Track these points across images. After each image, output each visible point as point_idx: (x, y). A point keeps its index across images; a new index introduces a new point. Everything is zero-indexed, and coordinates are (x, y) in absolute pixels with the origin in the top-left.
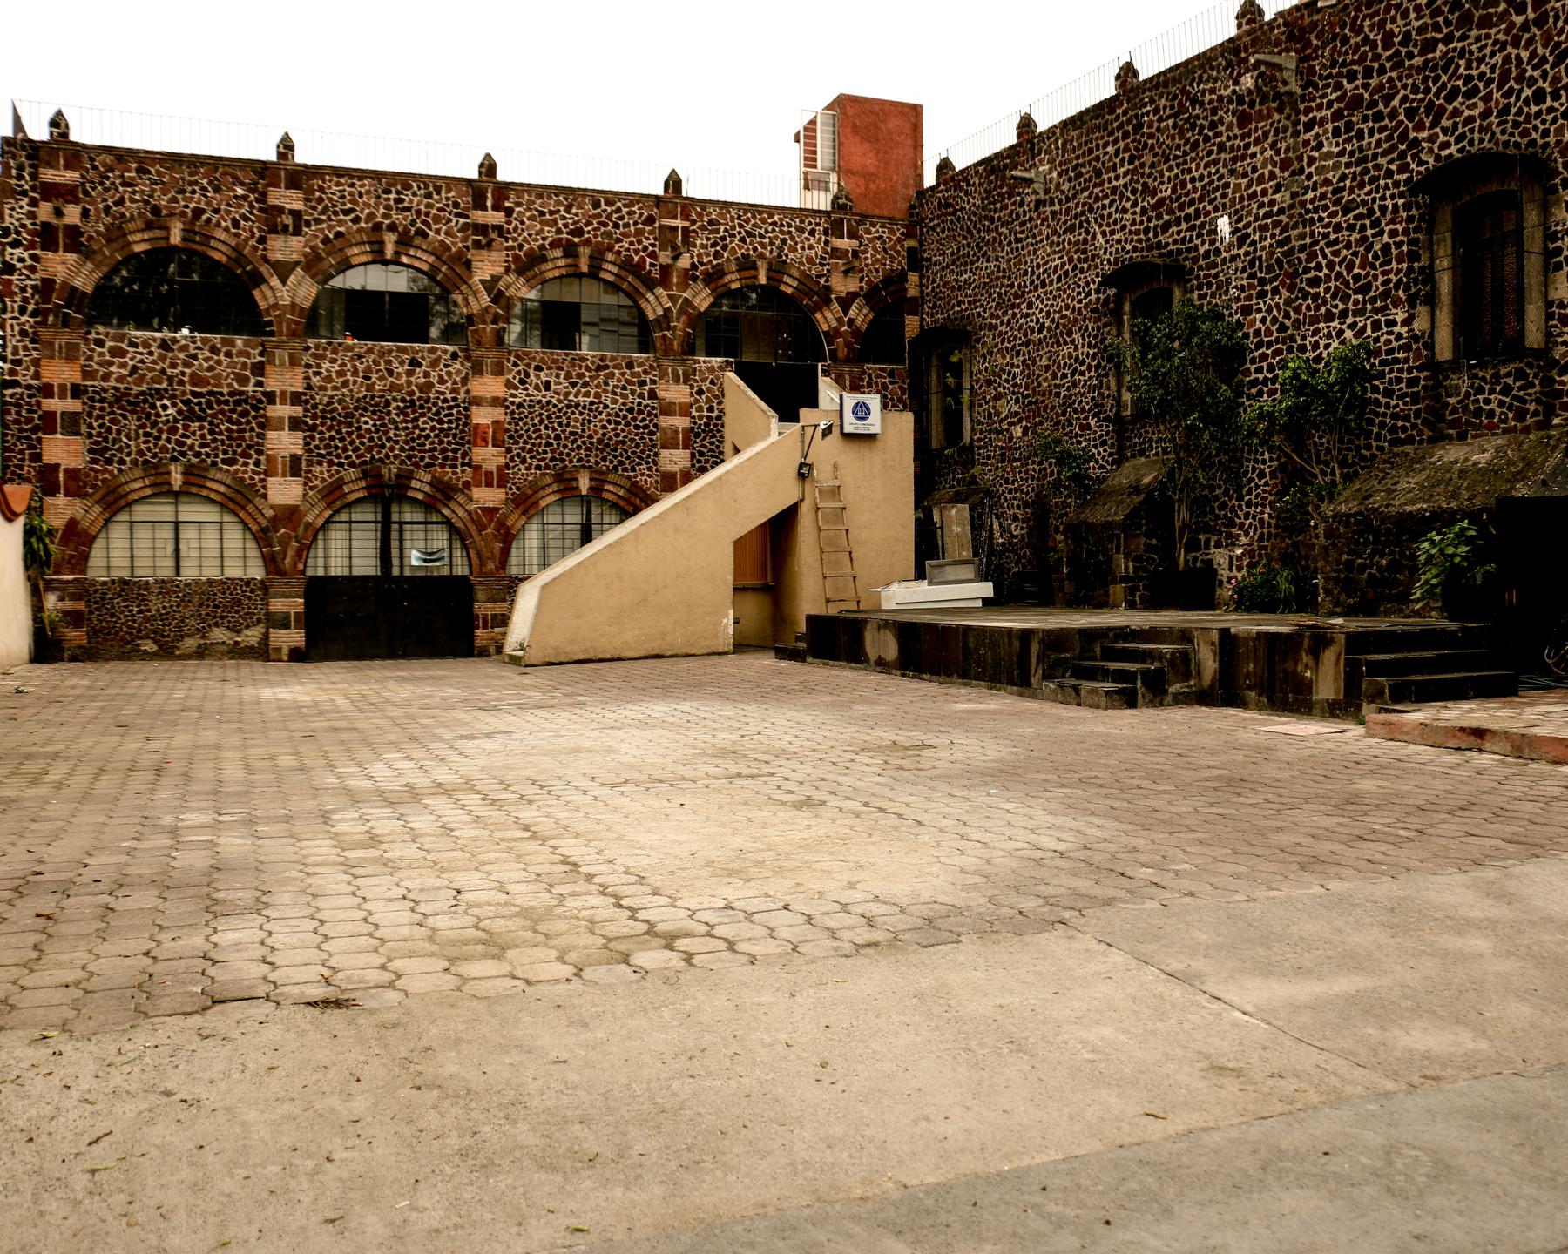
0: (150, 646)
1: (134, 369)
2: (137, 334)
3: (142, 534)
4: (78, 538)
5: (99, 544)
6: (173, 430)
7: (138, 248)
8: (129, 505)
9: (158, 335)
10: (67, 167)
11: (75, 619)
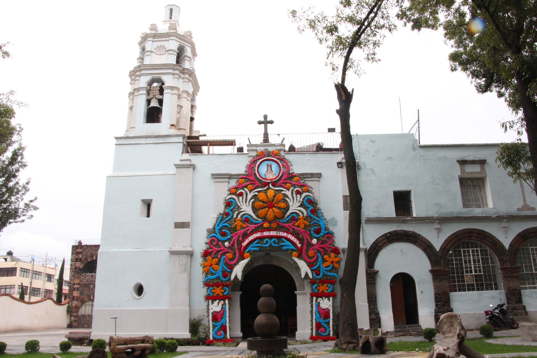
0: (86, 326)
1: (87, 280)
2: (88, 274)
3: (87, 307)
4: (77, 308)
5: (81, 308)
6: (92, 290)
7: (89, 261)
8: (86, 302)
9: (91, 274)
10: (80, 249)
11: (75, 321)
